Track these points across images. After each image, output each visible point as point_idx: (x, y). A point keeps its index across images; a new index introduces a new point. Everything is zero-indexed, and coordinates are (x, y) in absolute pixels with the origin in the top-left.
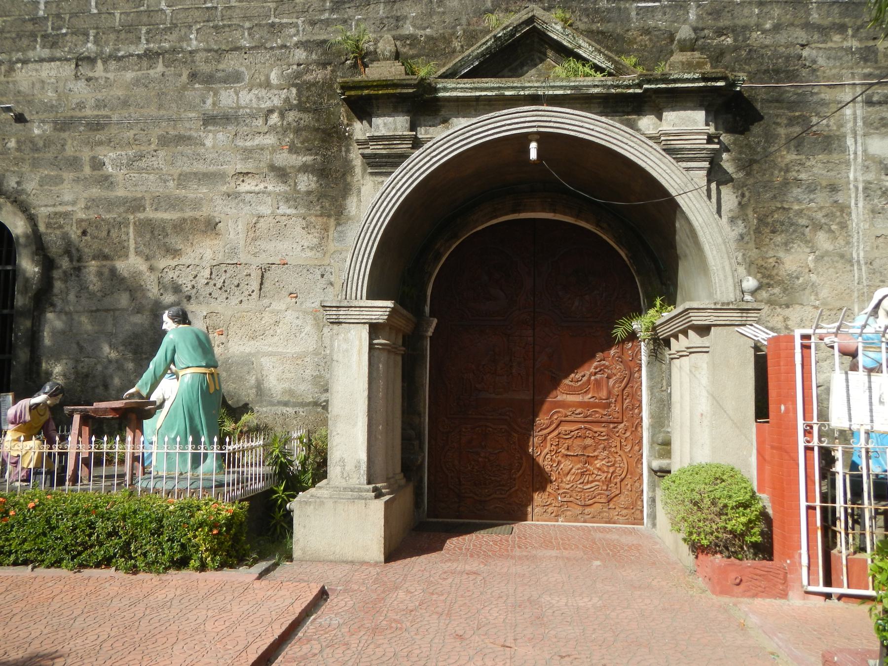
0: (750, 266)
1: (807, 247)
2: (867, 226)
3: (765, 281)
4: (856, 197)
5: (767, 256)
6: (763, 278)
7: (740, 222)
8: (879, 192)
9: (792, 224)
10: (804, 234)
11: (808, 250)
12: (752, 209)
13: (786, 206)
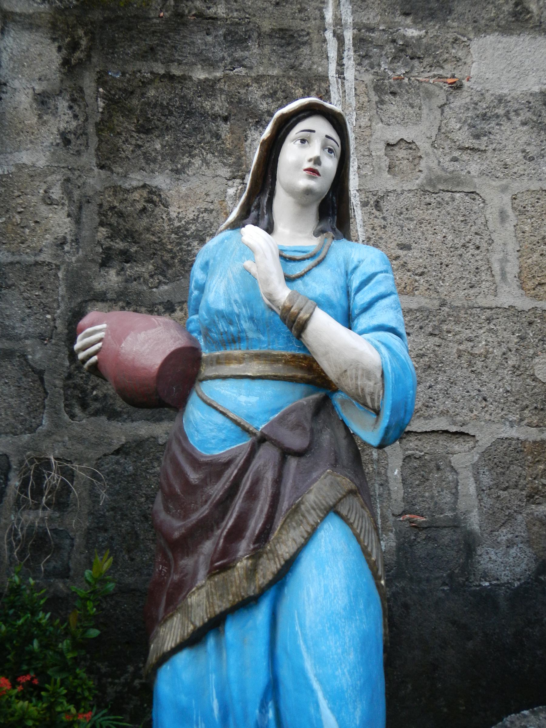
0: (80, 208)
1: (225, 164)
2: (364, 122)
3: (120, 245)
4: (340, 58)
5: (127, 186)
6: (111, 237)
7: (63, 104)
8: (390, 49)
9: (190, 114)
10: (218, 136)
11: (225, 172)
12: (94, 76)
13: (176, 71)
